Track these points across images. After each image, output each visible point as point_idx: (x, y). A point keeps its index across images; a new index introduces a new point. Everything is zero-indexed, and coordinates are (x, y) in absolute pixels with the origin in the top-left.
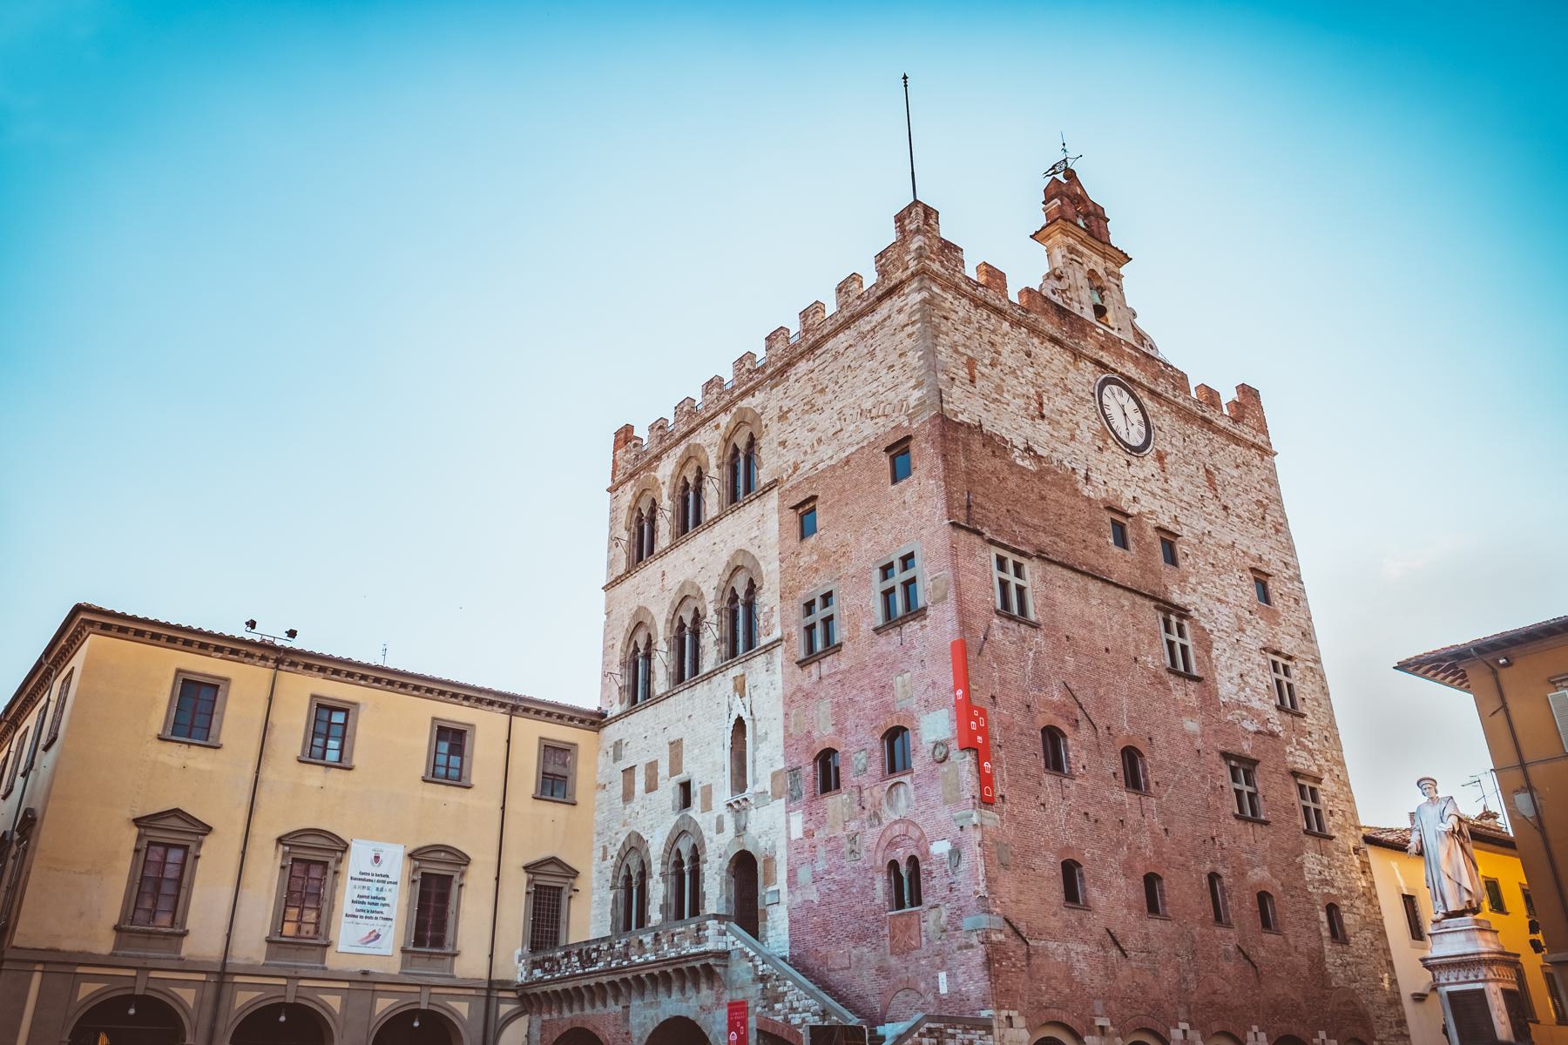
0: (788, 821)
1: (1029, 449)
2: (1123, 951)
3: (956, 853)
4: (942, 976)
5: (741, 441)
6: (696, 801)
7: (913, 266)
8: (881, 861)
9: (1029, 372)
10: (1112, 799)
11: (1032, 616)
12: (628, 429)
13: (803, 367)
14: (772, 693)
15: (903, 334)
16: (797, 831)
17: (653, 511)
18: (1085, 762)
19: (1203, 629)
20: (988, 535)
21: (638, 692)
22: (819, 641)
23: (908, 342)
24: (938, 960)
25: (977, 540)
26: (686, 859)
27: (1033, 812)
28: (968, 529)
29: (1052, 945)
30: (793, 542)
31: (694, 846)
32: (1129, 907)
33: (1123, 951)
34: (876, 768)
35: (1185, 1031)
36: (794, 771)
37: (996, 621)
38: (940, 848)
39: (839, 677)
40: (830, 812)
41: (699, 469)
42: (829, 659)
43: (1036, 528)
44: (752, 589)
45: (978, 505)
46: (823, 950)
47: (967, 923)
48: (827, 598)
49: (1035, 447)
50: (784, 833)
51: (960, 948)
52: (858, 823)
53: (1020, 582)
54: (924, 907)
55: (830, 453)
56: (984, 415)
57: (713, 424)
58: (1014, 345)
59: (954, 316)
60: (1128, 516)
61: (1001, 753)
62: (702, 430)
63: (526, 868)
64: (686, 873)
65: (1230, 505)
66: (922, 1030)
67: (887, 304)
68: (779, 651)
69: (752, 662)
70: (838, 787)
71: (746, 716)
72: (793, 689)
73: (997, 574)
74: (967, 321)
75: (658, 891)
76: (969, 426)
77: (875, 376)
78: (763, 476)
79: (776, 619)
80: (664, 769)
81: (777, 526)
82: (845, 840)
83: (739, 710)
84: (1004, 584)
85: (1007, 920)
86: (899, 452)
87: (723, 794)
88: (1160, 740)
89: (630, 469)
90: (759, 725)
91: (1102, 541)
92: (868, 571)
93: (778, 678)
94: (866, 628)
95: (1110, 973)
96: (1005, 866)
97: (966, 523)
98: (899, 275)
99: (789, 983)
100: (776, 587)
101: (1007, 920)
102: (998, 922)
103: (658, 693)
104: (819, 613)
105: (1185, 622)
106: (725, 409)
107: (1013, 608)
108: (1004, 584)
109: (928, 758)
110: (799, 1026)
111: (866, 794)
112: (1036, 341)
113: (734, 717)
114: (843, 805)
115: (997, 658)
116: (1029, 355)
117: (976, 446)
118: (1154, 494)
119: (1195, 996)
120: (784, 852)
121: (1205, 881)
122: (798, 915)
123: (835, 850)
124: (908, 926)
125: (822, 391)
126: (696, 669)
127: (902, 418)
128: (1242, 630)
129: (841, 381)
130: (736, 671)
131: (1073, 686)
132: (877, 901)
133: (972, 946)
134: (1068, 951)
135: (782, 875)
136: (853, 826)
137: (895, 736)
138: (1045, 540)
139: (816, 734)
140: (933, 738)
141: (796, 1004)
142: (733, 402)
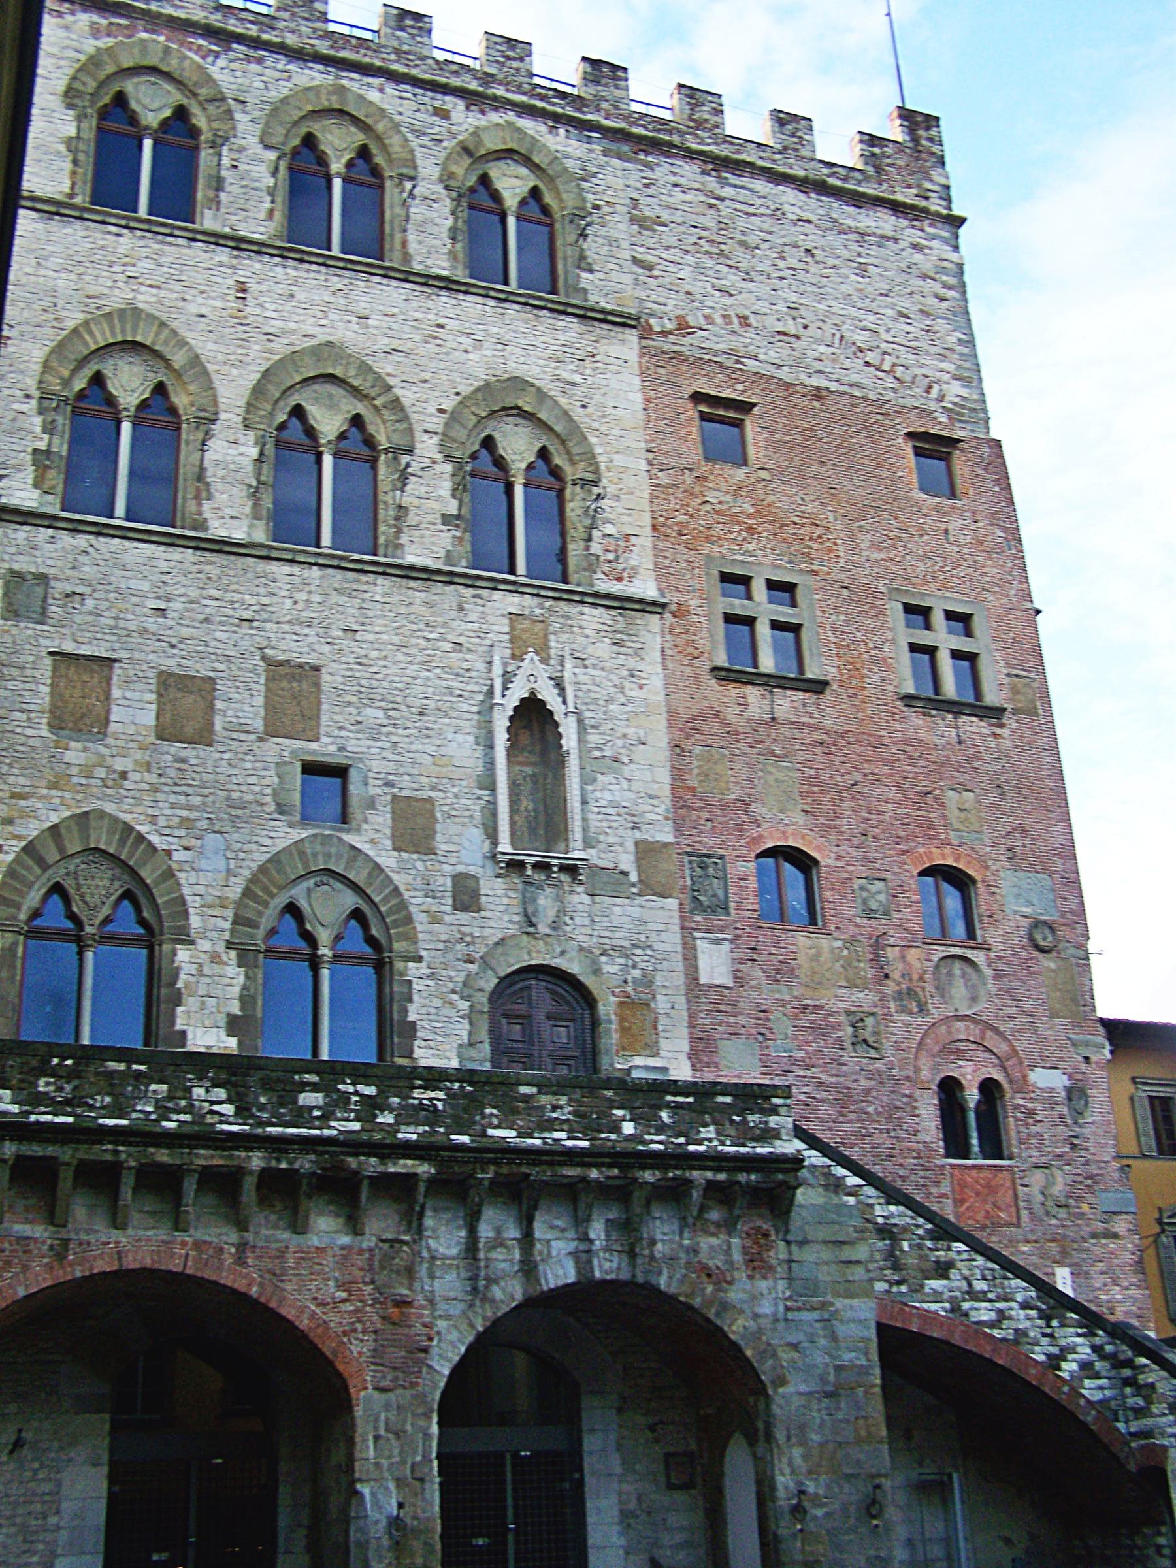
3: (1076, 1093)
8: (929, 1073)
13: (689, 171)
24: (1054, 1248)
30: (694, 453)
39: (818, 736)
51: (1094, 1235)
52: (873, 997)
55: (773, 356)
57: (427, 97)
81: (638, 398)
82: (843, 1018)
83: (531, 678)
90: (594, 738)
103: (217, 530)
109: (1020, 938)
110: (993, 1325)
113: (518, 693)
114: (835, 954)
124: (991, 1189)
132: (921, 1137)
141: (980, 1285)
142: (500, 104)
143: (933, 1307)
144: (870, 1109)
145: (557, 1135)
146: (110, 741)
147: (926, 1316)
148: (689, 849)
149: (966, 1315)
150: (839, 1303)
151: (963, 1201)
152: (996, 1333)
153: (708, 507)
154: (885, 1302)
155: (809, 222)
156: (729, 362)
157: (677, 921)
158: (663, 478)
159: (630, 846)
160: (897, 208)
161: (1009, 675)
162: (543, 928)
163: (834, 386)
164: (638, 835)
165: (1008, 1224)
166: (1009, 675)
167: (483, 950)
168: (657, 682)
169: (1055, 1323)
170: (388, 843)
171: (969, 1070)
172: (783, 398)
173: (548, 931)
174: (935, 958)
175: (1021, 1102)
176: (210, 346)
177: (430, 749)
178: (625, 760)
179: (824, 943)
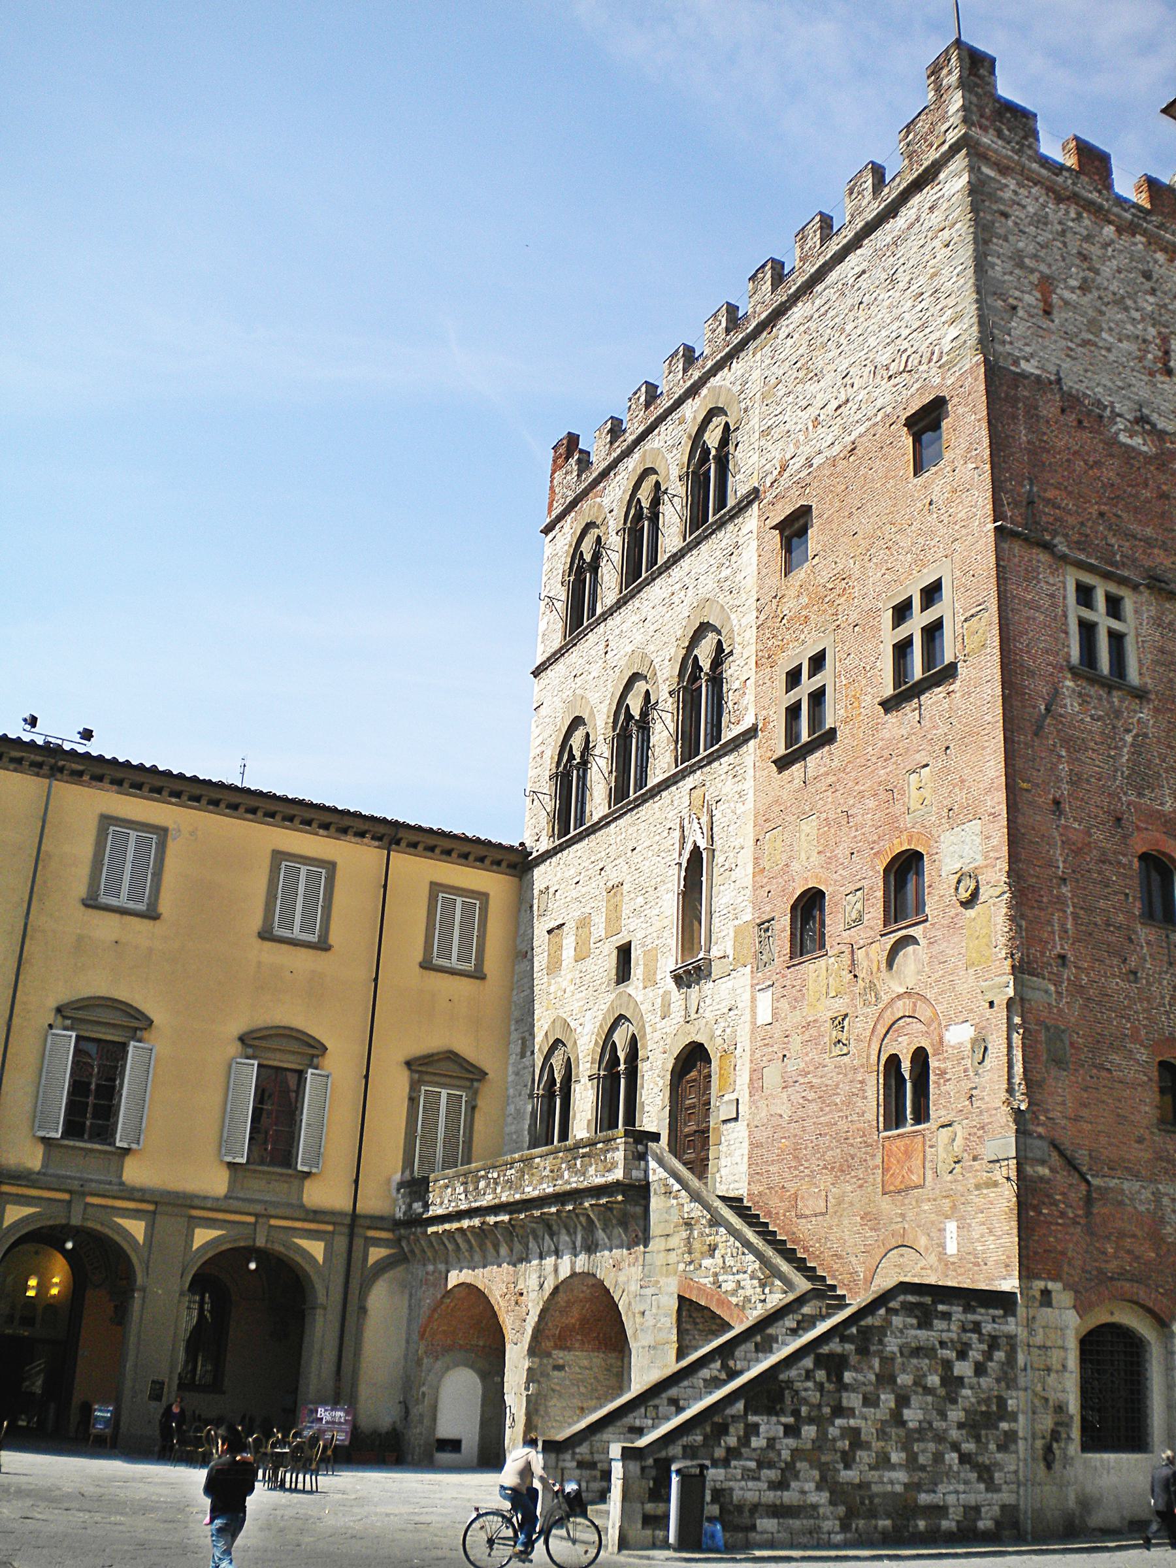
0: (753, 999)
1: (1142, 420)
4: (951, 1226)
5: (712, 439)
6: (637, 971)
7: (952, 137)
9: (1148, 303)
11: (1133, 676)
12: (572, 440)
13: (798, 312)
14: (740, 809)
15: (937, 243)
16: (764, 1016)
17: (597, 556)
20: (1063, 548)
21: (569, 821)
22: (807, 733)
23: (943, 253)
24: (946, 1204)
25: (1044, 557)
26: (622, 1055)
27: (1116, 984)
28: (1026, 540)
29: (1130, 1186)
30: (774, 580)
31: (634, 1035)
34: (875, 913)
36: (765, 926)
37: (1069, 683)
38: (959, 1035)
39: (831, 779)
40: (811, 984)
41: (657, 484)
42: (818, 754)
43: (1149, 542)
44: (720, 656)
45: (1048, 501)
46: (792, 1187)
47: (990, 1150)
48: (818, 662)
49: (1154, 417)
50: (747, 1017)
51: (978, 1187)
53: (1116, 625)
54: (932, 1125)
56: (1066, 365)
58: (1123, 261)
59: (1016, 212)
62: (662, 427)
63: (408, 1064)
64: (618, 1074)
66: (892, 1305)
67: (916, 200)
68: (752, 743)
69: (715, 764)
70: (822, 946)
71: (702, 844)
72: (770, 799)
73: (1074, 612)
74: (1041, 221)
75: (585, 1100)
76: (1038, 377)
77: (896, 312)
78: (738, 487)
79: (750, 697)
80: (599, 928)
82: (829, 1024)
84: (1088, 629)
85: (1055, 1146)
86: (927, 421)
87: (669, 962)
89: (571, 496)
90: (719, 858)
92: (876, 612)
93: (749, 785)
94: (870, 703)
96: (1059, 1062)
97: (1023, 528)
98: (933, 155)
99: (722, 1230)
100: (751, 650)
101: (1055, 1146)
102: (1039, 1148)
104: (808, 685)
106: (692, 391)
107: (1100, 667)
108: (1088, 629)
110: (734, 1293)
111: (860, 954)
112: (1160, 256)
113: (689, 847)
115: (1067, 742)
116: (1147, 275)
117: (1049, 408)
120: (747, 1049)
122: (762, 1135)
123: (813, 1041)
124: (908, 1154)
125: (824, 345)
126: (642, 781)
127: (934, 371)
129: (849, 328)
130: (690, 782)
133: (996, 1184)
135: (742, 1078)
136: (839, 1006)
137: (905, 869)
138: (1161, 560)
139: (795, 866)
140: (958, 866)
141: (730, 1261)
143: (703, 1281)
144: (838, 1100)
145: (545, 1186)
146: (562, 973)
147: (701, 1289)
148: (758, 921)
149: (720, 1287)
150: (663, 1281)
151: (888, 1170)
152: (734, 1300)
153: (784, 621)
154: (686, 1278)
155: (864, 272)
156: (802, 475)
157: (747, 980)
158: (762, 617)
159: (732, 934)
160: (917, 186)
161: (965, 621)
162: (694, 1016)
163: (862, 429)
164: (736, 922)
165: (916, 1187)
166: (965, 621)
167: (669, 1041)
168: (751, 792)
169: (767, 1290)
170: (641, 985)
171: (905, 1044)
172: (831, 474)
173: (696, 1016)
174: (889, 947)
175: (936, 1064)
176: (597, 695)
177: (656, 912)
178: (733, 866)
179: (822, 962)
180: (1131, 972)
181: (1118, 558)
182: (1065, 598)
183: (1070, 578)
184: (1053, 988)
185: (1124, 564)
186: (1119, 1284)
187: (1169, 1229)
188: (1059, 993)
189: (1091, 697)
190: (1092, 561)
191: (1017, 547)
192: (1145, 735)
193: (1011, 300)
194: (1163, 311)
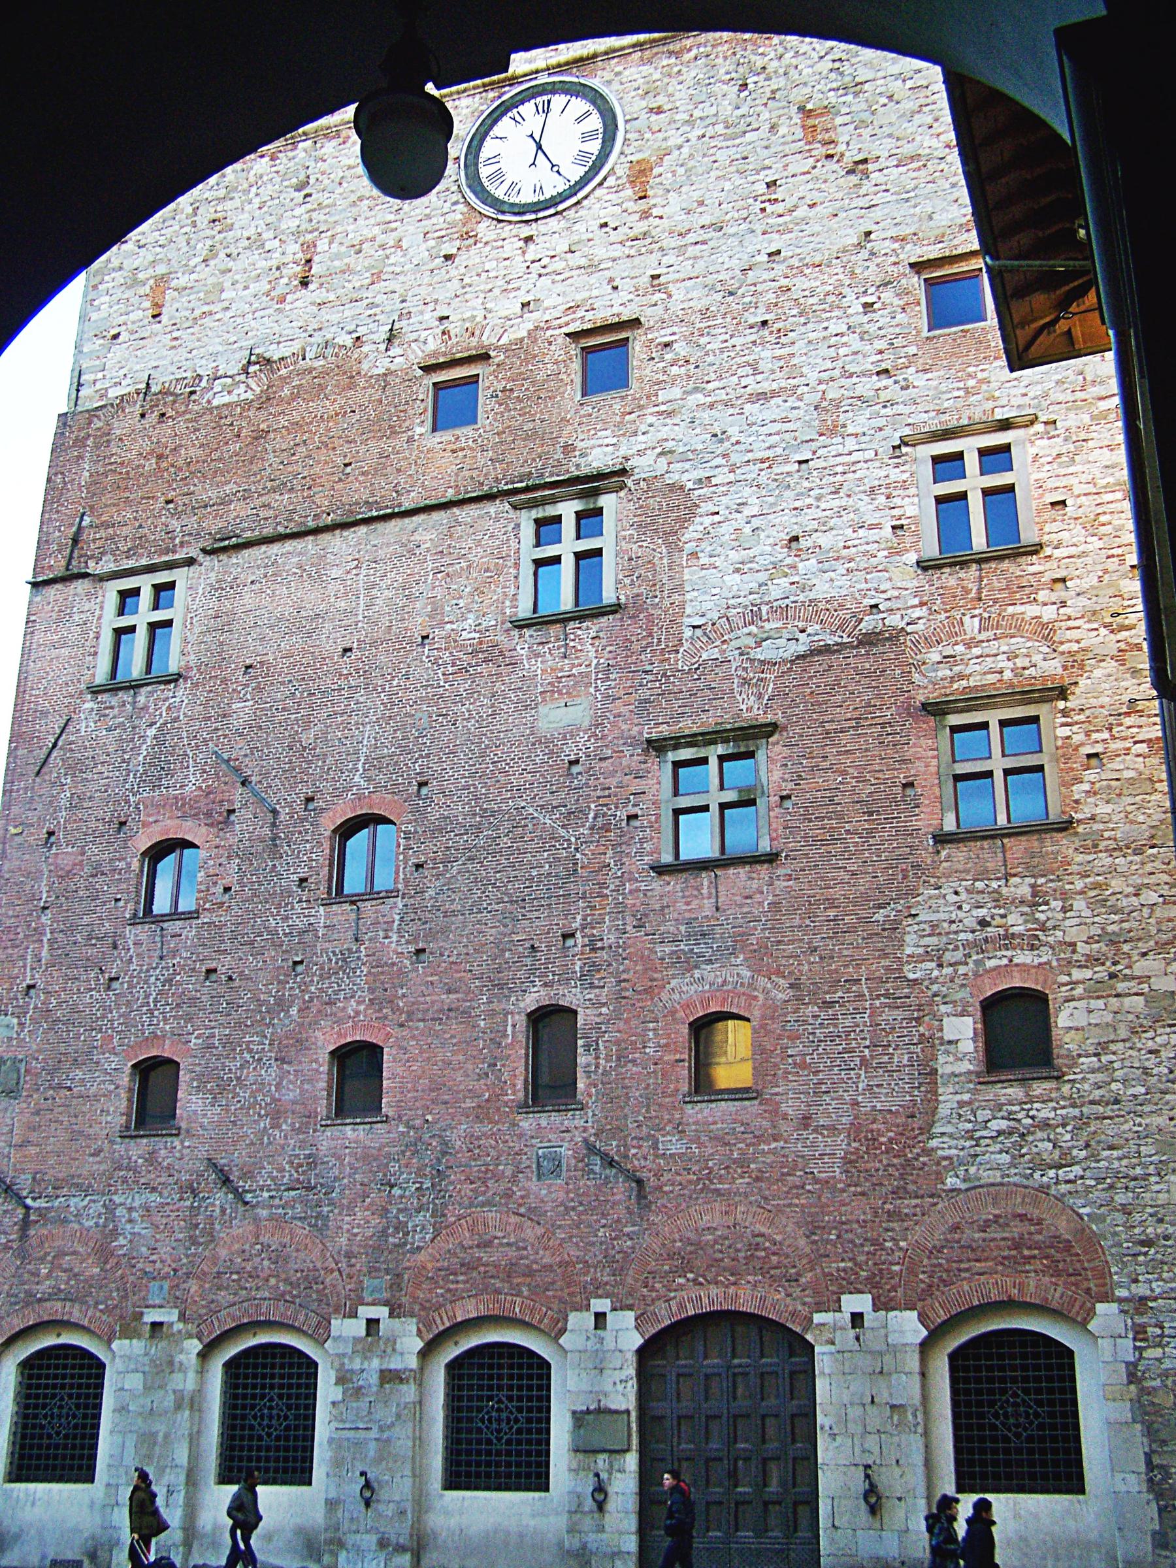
2: (239, 1195)
10: (283, 928)
18: (231, 879)
19: (677, 488)
25: (81, 586)
32: (276, 1115)
33: (239, 1195)
35: (372, 1323)
60: (485, 357)
61: (46, 919)
65: (881, 148)
88: (452, 773)
91: (400, 442)
95: (200, 1233)
105: (607, 502)
118: (592, 267)
119: (422, 1257)
121: (516, 1027)
128: (833, 430)
131: (240, 749)
134: (110, 1208)
180: (111, 979)
181: (177, 541)
182: (99, 618)
183: (111, 592)
184: (15, 1021)
185: (182, 544)
186: (48, 1304)
187: (122, 1241)
188: (21, 1024)
189: (112, 708)
190: (144, 562)
191: (52, 592)
192: (176, 719)
193: (114, 332)
194: (314, 215)
